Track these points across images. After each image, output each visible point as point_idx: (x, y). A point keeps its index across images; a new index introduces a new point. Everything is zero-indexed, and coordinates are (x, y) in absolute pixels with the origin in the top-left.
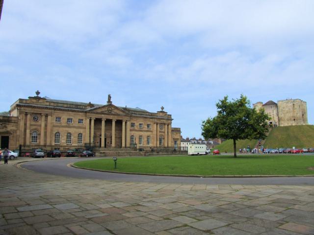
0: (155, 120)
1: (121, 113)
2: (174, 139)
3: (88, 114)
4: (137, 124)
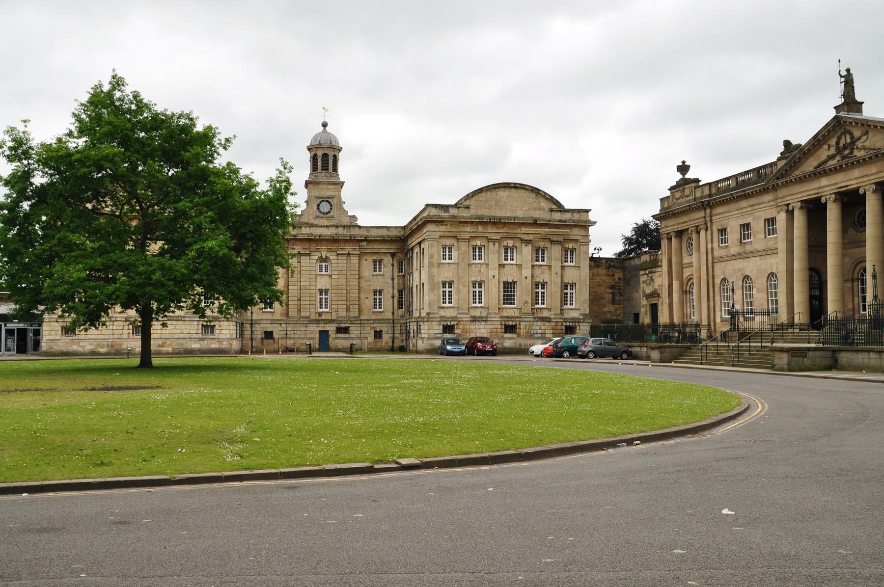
3: (782, 192)
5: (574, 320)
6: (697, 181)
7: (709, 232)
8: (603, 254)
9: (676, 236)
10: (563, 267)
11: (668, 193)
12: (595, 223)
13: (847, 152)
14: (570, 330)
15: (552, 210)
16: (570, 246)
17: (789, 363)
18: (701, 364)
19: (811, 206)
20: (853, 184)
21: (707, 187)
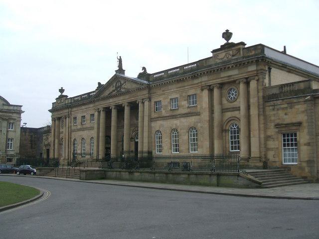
0: (205, 79)
1: (135, 86)
2: (277, 126)
3: (97, 103)
4: (165, 102)
5: (12, 155)
6: (67, 96)
7: (70, 119)
8: (28, 126)
9: (58, 120)
10: (7, 131)
11: (55, 101)
12: (24, 112)
13: (119, 89)
14: (10, 160)
15: (4, 105)
16: (12, 121)
17: (86, 176)
18: (55, 176)
19: (107, 110)
20: (120, 102)
21: (70, 99)
